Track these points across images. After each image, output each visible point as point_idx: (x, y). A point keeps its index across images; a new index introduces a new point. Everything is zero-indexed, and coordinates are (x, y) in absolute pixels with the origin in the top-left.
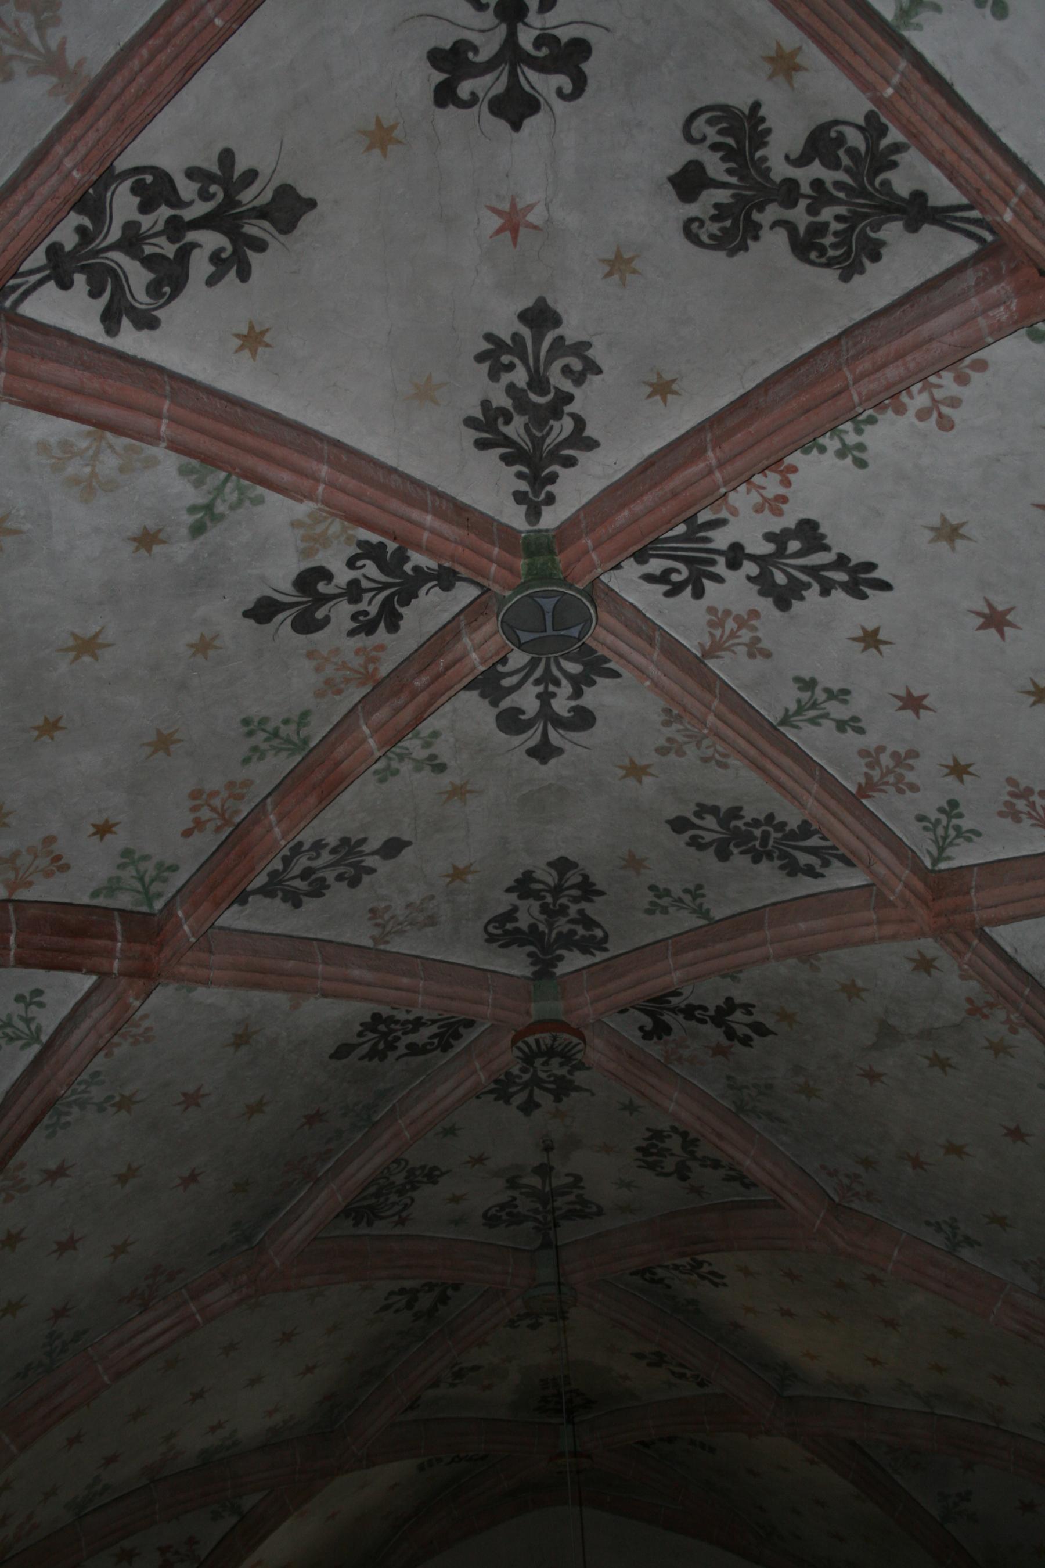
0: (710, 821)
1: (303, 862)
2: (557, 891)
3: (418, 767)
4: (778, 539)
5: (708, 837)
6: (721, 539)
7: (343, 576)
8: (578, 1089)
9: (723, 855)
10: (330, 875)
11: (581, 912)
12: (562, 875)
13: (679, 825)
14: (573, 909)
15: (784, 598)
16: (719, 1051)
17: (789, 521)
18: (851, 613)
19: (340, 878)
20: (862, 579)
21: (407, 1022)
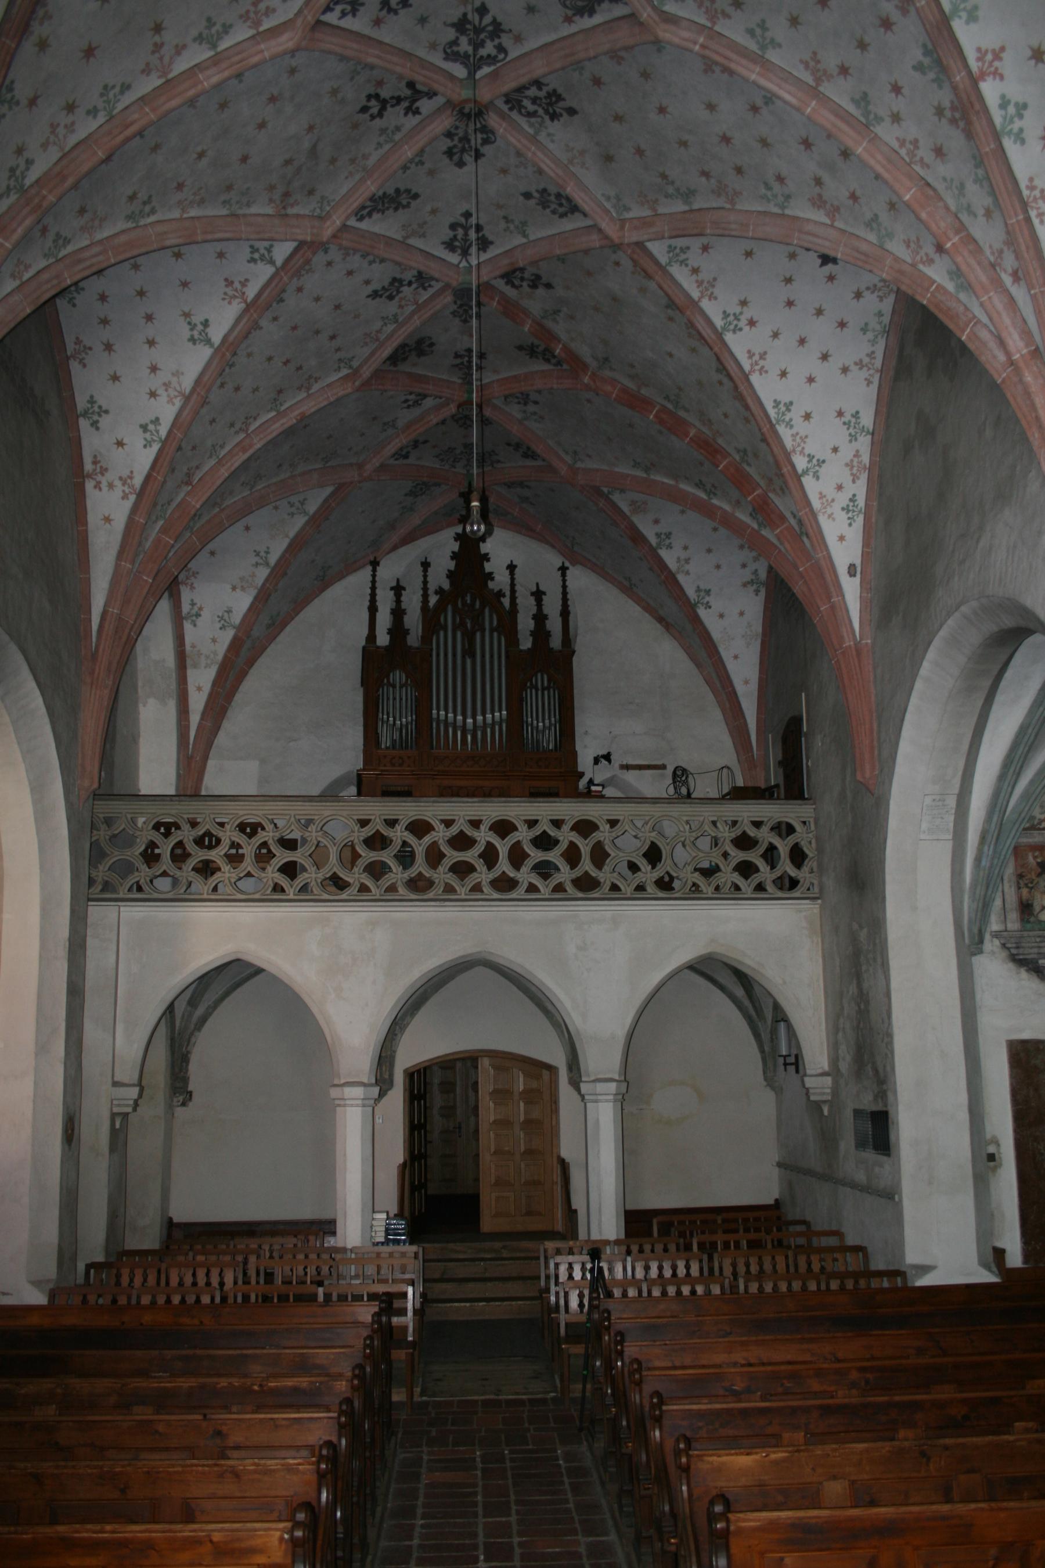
0: (404, 202)
1: (561, 210)
2: (463, 150)
3: (512, 221)
4: (398, 292)
5: (404, 195)
6: (414, 286)
7: (525, 284)
8: (453, 25)
9: (397, 191)
10: (552, 198)
11: (452, 140)
12: (461, 159)
13: (416, 196)
14: (456, 142)
15: (394, 280)
16: (380, 83)
17: (397, 299)
18: (375, 286)
19: (549, 195)
20: (375, 295)
21: (540, 105)
